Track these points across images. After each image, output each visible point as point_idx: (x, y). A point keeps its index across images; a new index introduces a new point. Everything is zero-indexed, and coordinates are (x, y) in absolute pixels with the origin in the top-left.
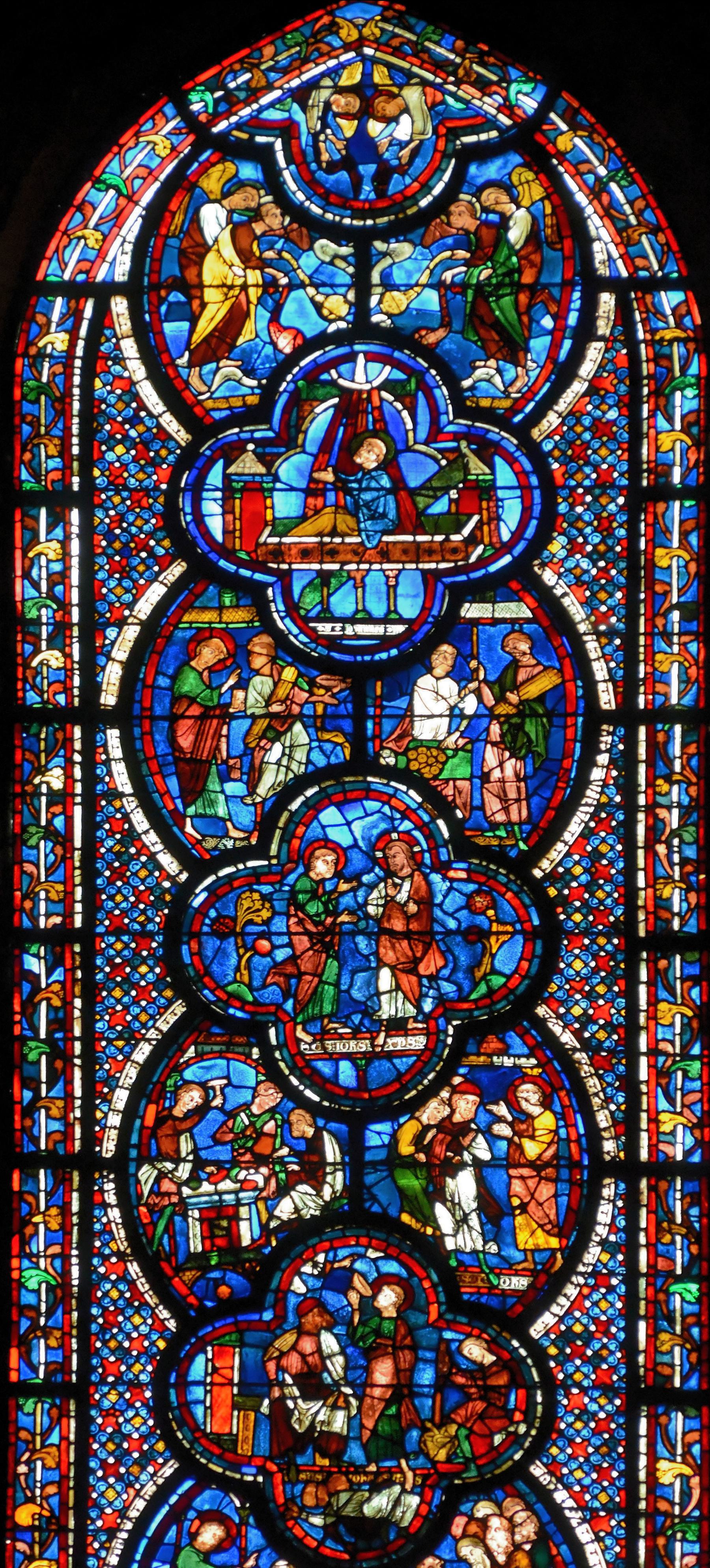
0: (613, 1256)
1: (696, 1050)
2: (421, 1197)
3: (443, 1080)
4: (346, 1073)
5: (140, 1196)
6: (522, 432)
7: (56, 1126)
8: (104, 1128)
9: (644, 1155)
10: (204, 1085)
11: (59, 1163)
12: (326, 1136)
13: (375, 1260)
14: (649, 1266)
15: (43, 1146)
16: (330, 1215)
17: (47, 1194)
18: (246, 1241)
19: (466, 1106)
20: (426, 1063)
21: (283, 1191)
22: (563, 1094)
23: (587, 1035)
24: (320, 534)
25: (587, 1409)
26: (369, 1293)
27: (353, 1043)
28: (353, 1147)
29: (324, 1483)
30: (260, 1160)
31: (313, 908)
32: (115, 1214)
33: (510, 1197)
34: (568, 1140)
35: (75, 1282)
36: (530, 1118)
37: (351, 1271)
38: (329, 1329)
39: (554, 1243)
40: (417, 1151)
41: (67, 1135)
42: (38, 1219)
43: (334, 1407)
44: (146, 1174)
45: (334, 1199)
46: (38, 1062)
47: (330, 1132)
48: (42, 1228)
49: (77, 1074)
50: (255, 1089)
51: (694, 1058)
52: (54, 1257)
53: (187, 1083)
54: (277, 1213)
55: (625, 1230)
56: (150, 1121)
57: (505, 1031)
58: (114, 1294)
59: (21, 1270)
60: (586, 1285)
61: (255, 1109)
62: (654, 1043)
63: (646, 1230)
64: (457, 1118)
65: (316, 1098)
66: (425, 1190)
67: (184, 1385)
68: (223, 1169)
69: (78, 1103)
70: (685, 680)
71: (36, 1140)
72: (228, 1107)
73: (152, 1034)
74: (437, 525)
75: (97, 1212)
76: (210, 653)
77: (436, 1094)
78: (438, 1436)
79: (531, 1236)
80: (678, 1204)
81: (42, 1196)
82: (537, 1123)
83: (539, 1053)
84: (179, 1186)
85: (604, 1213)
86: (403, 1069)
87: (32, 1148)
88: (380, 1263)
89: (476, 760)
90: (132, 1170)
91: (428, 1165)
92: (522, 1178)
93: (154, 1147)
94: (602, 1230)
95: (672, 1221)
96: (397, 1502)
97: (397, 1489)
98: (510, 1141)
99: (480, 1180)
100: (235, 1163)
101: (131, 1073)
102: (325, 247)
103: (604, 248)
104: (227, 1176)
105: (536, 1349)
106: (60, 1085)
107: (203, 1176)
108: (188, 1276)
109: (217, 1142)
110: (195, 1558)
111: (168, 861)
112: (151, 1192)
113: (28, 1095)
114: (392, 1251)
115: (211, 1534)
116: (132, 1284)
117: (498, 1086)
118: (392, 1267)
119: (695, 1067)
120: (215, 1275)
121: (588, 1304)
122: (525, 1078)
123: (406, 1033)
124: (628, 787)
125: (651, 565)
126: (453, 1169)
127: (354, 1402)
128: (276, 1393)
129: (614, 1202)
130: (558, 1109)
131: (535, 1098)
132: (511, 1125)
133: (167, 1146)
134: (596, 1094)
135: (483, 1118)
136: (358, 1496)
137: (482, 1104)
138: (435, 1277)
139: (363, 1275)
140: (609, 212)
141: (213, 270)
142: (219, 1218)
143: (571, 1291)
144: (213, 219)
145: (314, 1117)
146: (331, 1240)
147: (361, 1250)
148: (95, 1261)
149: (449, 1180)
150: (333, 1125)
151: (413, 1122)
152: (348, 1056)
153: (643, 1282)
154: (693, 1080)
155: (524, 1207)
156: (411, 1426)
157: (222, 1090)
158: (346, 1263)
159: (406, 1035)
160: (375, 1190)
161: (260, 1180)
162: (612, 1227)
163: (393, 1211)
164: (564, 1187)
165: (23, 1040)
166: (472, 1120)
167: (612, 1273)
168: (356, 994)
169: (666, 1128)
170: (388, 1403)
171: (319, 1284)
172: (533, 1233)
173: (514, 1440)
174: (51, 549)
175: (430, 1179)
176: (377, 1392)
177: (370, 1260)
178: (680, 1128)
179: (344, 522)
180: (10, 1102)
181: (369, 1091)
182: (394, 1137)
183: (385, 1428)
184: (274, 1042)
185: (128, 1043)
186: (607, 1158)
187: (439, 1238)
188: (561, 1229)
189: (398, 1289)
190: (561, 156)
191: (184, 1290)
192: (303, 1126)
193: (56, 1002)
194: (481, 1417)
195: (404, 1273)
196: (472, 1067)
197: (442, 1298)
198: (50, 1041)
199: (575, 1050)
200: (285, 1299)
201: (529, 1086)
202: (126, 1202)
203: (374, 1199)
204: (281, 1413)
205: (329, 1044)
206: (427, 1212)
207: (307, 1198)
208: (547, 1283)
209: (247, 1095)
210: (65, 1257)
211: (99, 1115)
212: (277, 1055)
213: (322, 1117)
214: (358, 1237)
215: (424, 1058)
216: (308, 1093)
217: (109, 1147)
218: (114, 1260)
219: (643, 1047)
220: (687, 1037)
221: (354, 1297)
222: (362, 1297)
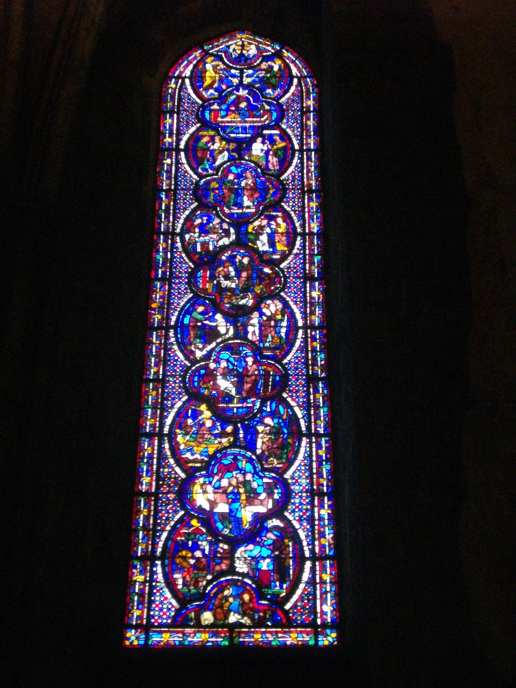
3: (259, 217)
5: (185, 240)
6: (277, 101)
16: (231, 243)
19: (265, 222)
21: (220, 239)
24: (231, 118)
25: (295, 283)
26: (241, 259)
29: (229, 298)
30: (214, 233)
31: (228, 185)
36: (279, 224)
38: (231, 266)
43: (232, 282)
44: (187, 236)
67: (196, 278)
70: (314, 144)
74: (257, 117)
76: (205, 139)
78: (258, 288)
89: (267, 158)
96: (247, 301)
97: (247, 299)
101: (184, 216)
102: (233, 71)
103: (295, 71)
105: (282, 270)
110: (197, 314)
111: (195, 176)
113: (159, 221)
115: (201, 309)
116: (182, 258)
123: (251, 209)
124: (302, 163)
125: (306, 125)
126: (261, 234)
127: (237, 281)
128: (218, 279)
133: (192, 230)
136: (238, 300)
140: (296, 65)
141: (208, 74)
142: (205, 245)
144: (209, 67)
155: (278, 242)
156: (251, 286)
168: (239, 201)
170: (246, 281)
173: (277, 288)
174: (170, 122)
176: (243, 279)
179: (237, 116)
183: (245, 286)
187: (258, 248)
190: (285, 57)
193: (167, 203)
194: (269, 283)
204: (219, 283)
208: (284, 257)
211: (176, 225)
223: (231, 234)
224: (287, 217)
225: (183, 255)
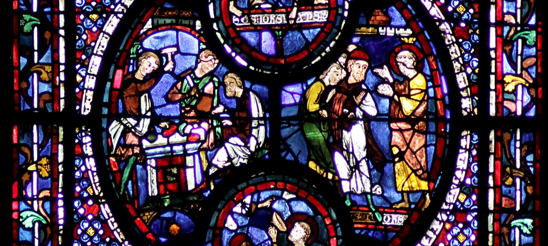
0: (469, 197)
1: (533, 21)
2: (324, 147)
4: (267, 42)
5: (110, 148)
7: (45, 88)
8: (82, 90)
9: (492, 111)
10: (158, 53)
11: (48, 120)
12: (252, 96)
13: (289, 201)
14: (495, 204)
15: (36, 106)
17: (39, 146)
18: (191, 186)
19: (358, 70)
20: (328, 34)
21: (220, 143)
22: (431, 59)
23: (450, 9)
26: (284, 229)
27: (272, 16)
28: (272, 104)
30: (202, 116)
32: (91, 163)
33: (391, 147)
34: (435, 98)
35: (61, 222)
36: (407, 80)
37: (271, 210)
39: (424, 185)
40: (321, 108)
41: (54, 96)
42: (32, 168)
44: (115, 129)
45: (258, 149)
46: (32, 32)
47: (255, 93)
48: (35, 175)
49: (62, 43)
50: (198, 56)
51: (532, 28)
52: (45, 199)
53: (146, 50)
54: (214, 162)
55: (477, 174)
56: (118, 84)
57: (388, 6)
58: (91, 232)
59: (20, 212)
60: (448, 221)
61: (198, 73)
62: (501, 14)
63: (494, 174)
64: (351, 80)
65: (245, 64)
66: (327, 141)
68: (174, 125)
69: (62, 68)
71: (30, 100)
72: (177, 71)
73: (119, 8)
75: (77, 162)
77: (336, 60)
79: (408, 180)
80: (518, 151)
81: (35, 147)
82: (412, 84)
83: (414, 25)
84: (140, 139)
85: (462, 160)
86: (310, 38)
87: (28, 107)
88: (293, 203)
90: (104, 125)
91: (329, 120)
92: (401, 131)
93: (121, 106)
94: (460, 175)
95: (513, 166)
98: (391, 99)
99: (369, 133)
100: (182, 118)
101: (103, 42)
104: (177, 131)
106: (48, 53)
107: (159, 130)
108: (147, 216)
109: (169, 101)
112: (119, 144)
113: (24, 61)
114: (303, 194)
116: (104, 223)
117: (381, 53)
118: (301, 207)
119: (532, 36)
120: (168, 215)
121: (449, 237)
122: (404, 46)
126: (348, 123)
129: (470, 151)
130: (428, 72)
131: (410, 63)
132: (392, 85)
134: (457, 60)
135: (371, 80)
137: (370, 68)
138: (334, 215)
139: (280, 214)
142: (172, 165)
143: (437, 226)
145: (243, 80)
146: (255, 185)
147: (278, 192)
148: (76, 204)
149: (345, 132)
150: (257, 87)
151: (318, 83)
152: (269, 28)
153: (491, 218)
154: (530, 47)
155: (401, 155)
157: (173, 56)
158: (267, 204)
159: (313, 10)
160: (289, 142)
161: (201, 133)
162: (468, 171)
163: (302, 159)
164: (432, 139)
165: (20, 13)
166: (363, 82)
167: (468, 211)
169: (510, 88)
171: (246, 222)
172: (409, 177)
175: (331, 132)
177: (285, 203)
178: (520, 87)
180: (11, 67)
181: (285, 57)
182: (304, 96)
184: (212, 16)
185: (100, 17)
186: (465, 113)
188: (429, 174)
189: (306, 225)
191: (144, 229)
192: (234, 87)
195: (311, 212)
196: (363, 37)
197: (340, 234)
198: (40, 14)
199: (441, 21)
200: (221, 235)
201: (406, 53)
202: (100, 154)
203: (289, 150)
205: (254, 17)
206: (328, 160)
207: (237, 149)
209: (192, 61)
210: (53, 200)
211: (79, 78)
212: (215, 26)
213: (249, 80)
214: (276, 182)
215: (327, 28)
216: (239, 59)
217: (86, 107)
218: (90, 202)
219: (493, 20)
220: (525, 10)
221: (273, 233)
222: (279, 232)
223: (254, 123)
224: (432, 52)
225: (106, 210)
